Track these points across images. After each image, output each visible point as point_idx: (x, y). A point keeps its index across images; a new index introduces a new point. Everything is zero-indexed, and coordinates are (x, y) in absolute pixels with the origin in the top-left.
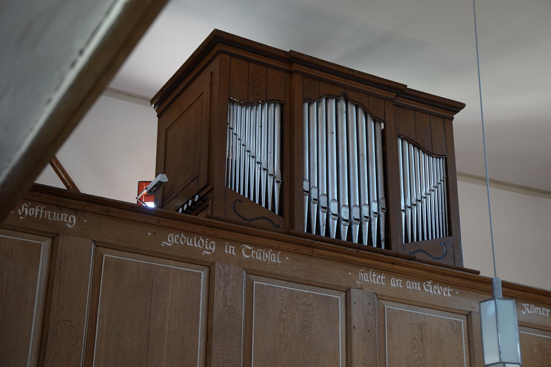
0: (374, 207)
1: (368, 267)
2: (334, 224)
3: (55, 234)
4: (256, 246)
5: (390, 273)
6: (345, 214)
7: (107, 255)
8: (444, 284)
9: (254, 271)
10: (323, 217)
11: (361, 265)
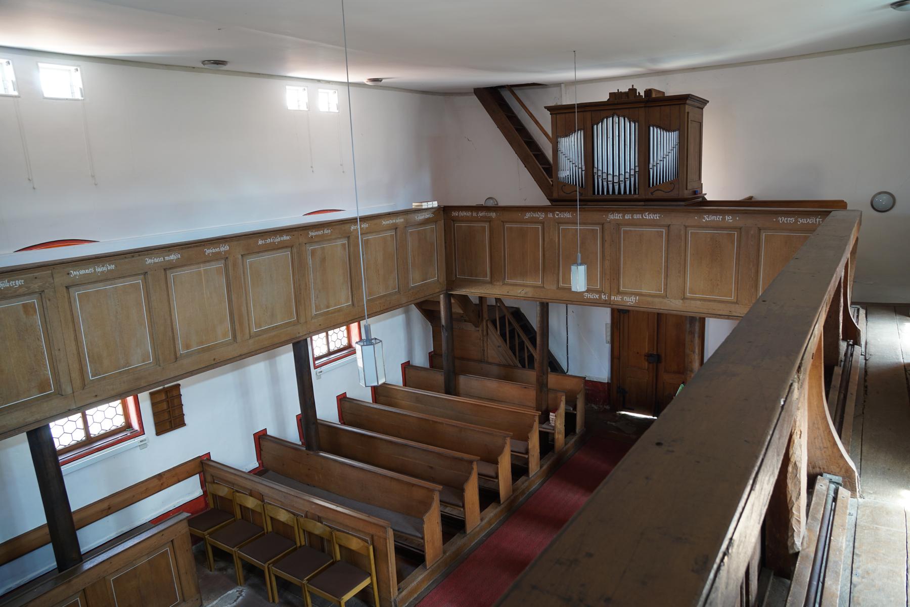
0: (632, 172)
1: (613, 211)
3: (489, 220)
4: (560, 212)
5: (625, 211)
6: (616, 180)
7: (507, 225)
8: (654, 212)
9: (560, 222)
10: (605, 183)
11: (609, 211)
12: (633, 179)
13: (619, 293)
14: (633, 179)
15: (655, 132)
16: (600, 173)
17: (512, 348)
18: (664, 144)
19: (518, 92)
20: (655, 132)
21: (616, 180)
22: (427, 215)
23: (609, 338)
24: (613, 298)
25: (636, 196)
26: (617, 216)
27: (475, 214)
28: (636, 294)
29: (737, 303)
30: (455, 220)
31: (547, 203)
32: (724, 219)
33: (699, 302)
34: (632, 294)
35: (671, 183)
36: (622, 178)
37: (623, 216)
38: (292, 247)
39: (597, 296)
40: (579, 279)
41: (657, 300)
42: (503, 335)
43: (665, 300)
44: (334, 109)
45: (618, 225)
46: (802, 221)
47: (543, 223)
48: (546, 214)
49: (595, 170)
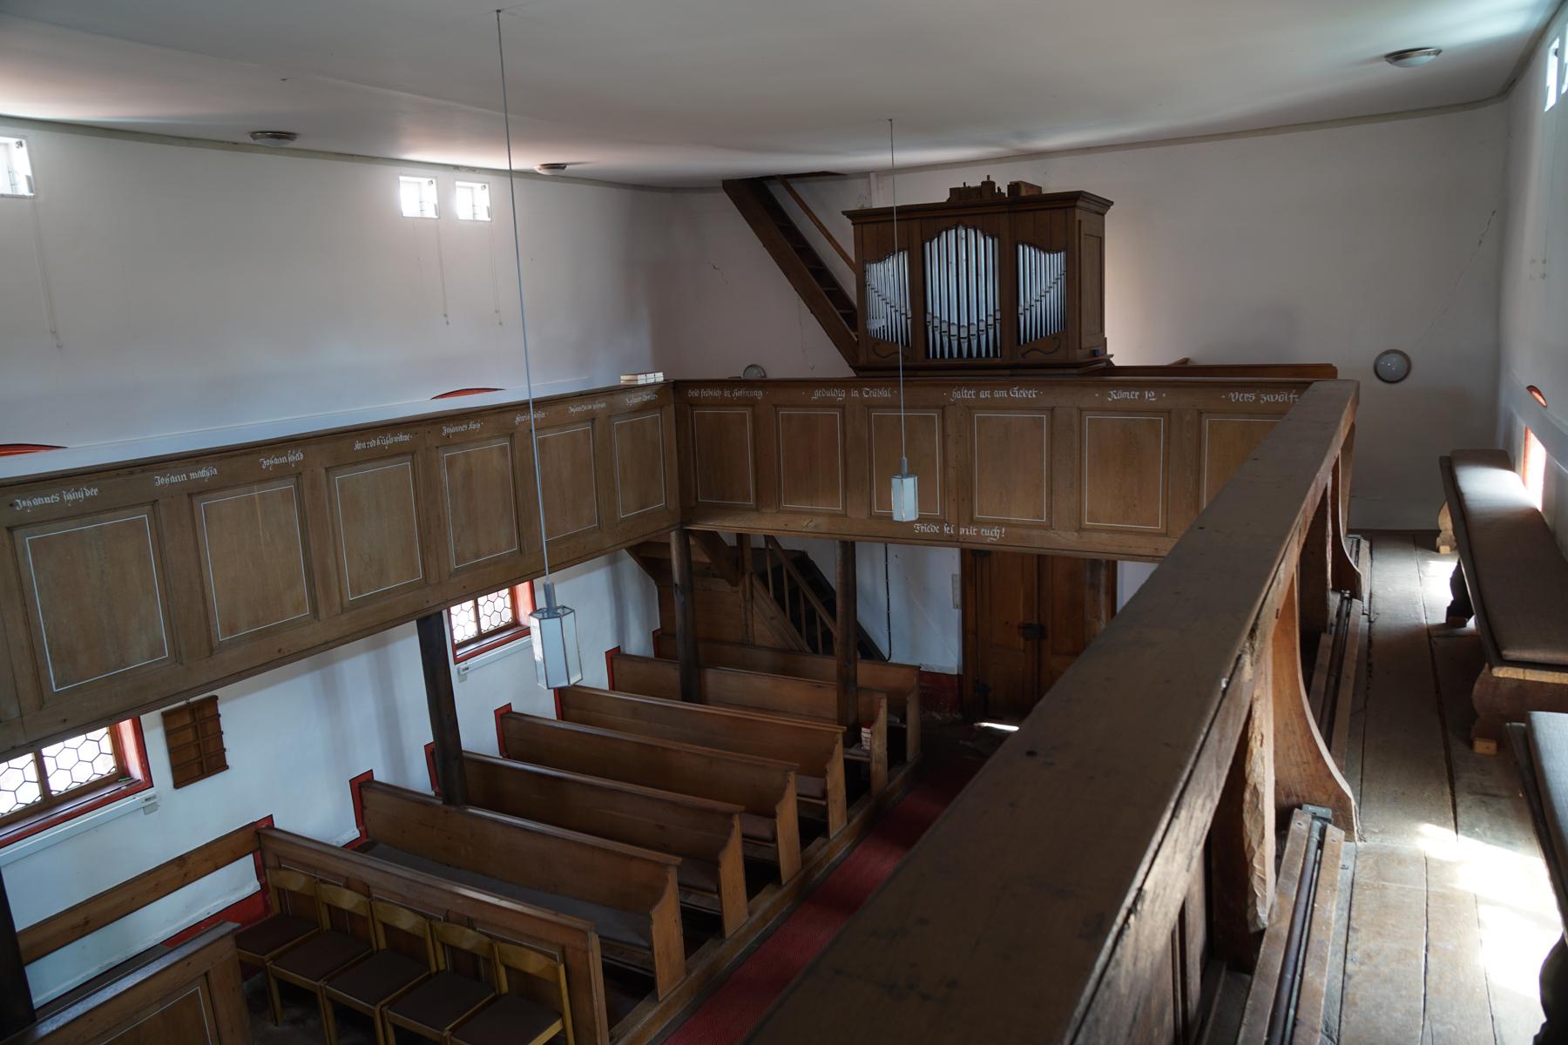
0: (991, 321)
1: (960, 386)
2: (955, 344)
3: (752, 404)
4: (872, 387)
5: (979, 387)
6: (964, 334)
8: (1029, 386)
9: (870, 406)
10: (946, 339)
12: (991, 332)
13: (972, 522)
14: (991, 332)
15: (1026, 254)
16: (937, 322)
17: (795, 620)
18: (1042, 275)
19: (799, 187)
20: (1026, 254)
21: (964, 334)
22: (646, 397)
23: (958, 600)
24: (962, 531)
25: (997, 361)
26: (967, 394)
27: (727, 393)
28: (1000, 524)
29: (1166, 535)
30: (694, 403)
31: (851, 373)
32: (1142, 396)
33: (1104, 536)
34: (991, 524)
35: (1055, 337)
36: (973, 330)
37: (977, 394)
38: (413, 453)
39: (936, 529)
40: (905, 500)
41: (1035, 532)
42: (779, 599)
43: (1051, 534)
44: (483, 216)
45: (969, 407)
46: (1267, 398)
47: (842, 407)
48: (848, 393)
49: (929, 318)
